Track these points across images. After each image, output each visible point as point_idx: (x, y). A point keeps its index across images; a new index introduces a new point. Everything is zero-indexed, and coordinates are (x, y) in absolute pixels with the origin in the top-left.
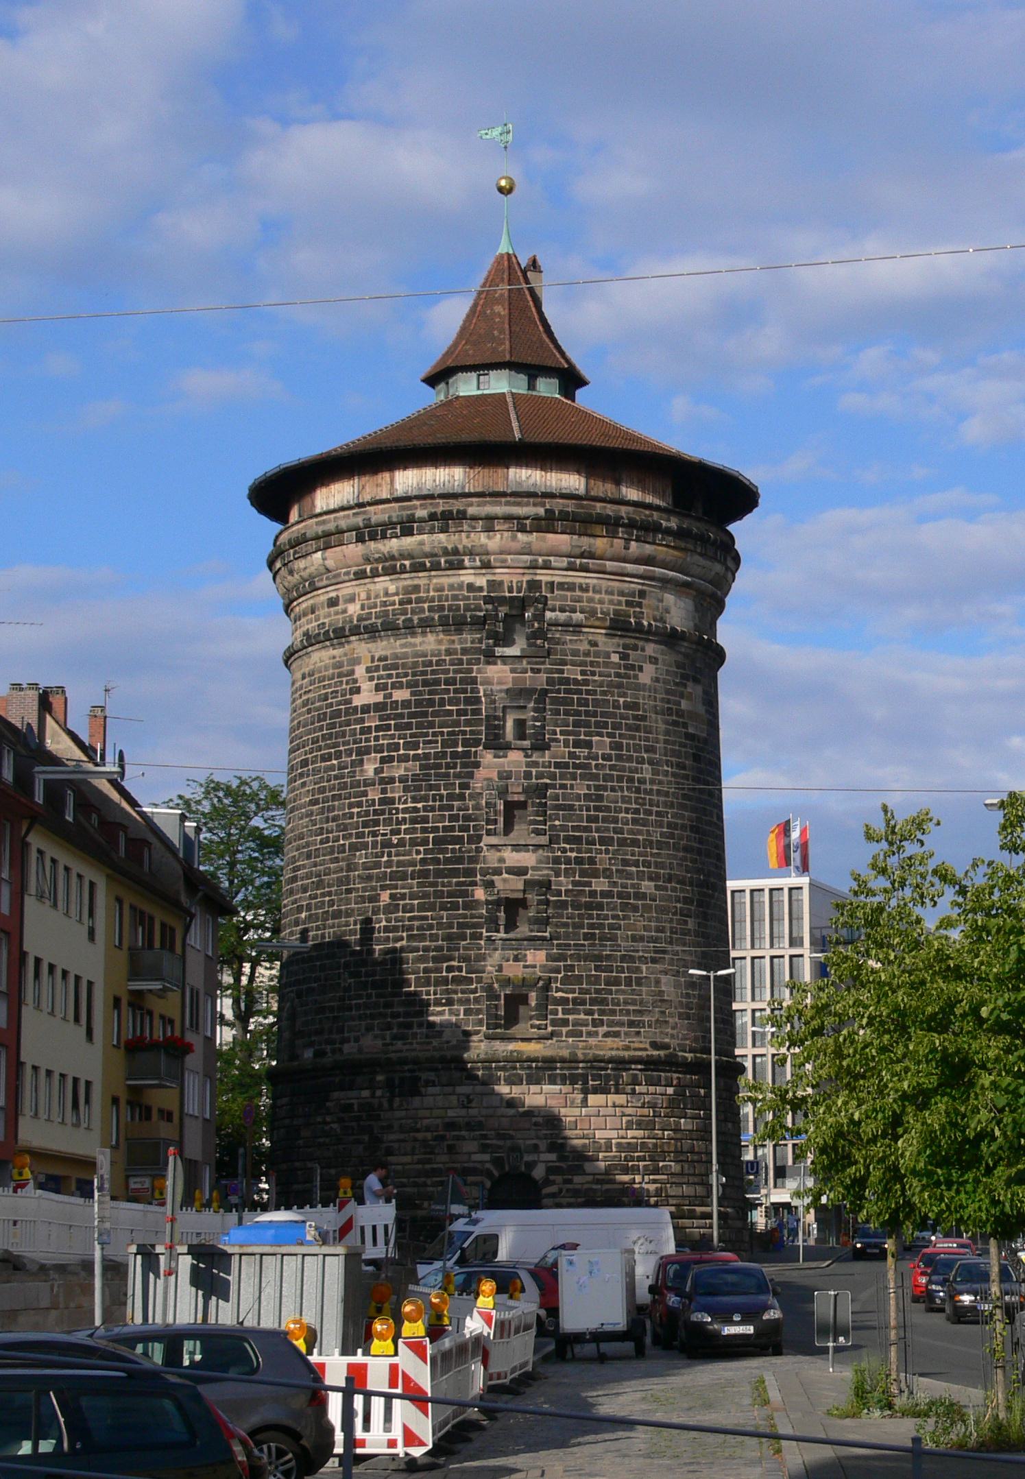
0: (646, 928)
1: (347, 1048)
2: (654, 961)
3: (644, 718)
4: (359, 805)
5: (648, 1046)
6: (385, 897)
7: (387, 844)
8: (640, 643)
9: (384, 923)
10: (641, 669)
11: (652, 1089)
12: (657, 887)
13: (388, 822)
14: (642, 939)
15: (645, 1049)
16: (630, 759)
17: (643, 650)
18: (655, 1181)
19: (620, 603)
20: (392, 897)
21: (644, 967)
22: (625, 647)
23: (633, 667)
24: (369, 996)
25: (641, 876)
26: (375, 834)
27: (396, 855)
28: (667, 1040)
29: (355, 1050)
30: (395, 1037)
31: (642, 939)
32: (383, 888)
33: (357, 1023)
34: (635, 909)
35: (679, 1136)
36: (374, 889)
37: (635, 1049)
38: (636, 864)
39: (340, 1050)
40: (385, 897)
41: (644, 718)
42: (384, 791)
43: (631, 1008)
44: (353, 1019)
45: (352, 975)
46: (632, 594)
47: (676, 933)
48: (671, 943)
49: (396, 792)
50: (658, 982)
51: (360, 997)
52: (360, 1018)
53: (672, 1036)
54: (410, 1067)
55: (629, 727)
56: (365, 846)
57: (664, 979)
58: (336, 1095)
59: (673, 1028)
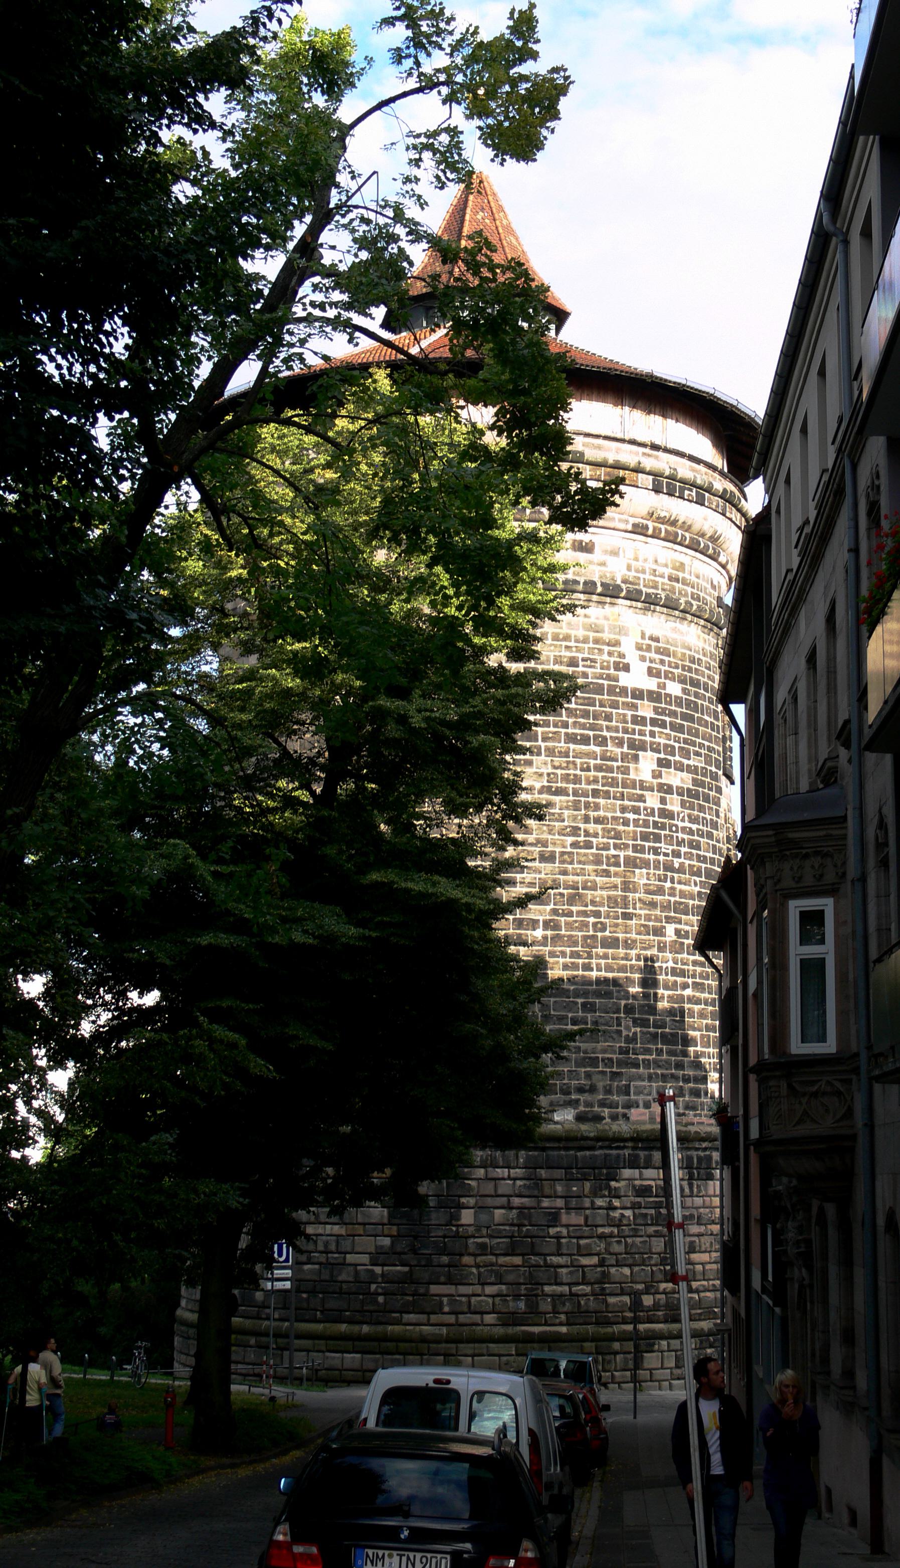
1: (635, 1114)
4: (636, 810)
6: (670, 929)
7: (669, 867)
9: (671, 964)
13: (669, 840)
20: (678, 932)
24: (659, 1052)
26: (656, 851)
27: (680, 883)
29: (647, 1117)
30: (687, 1107)
32: (669, 920)
33: (646, 1083)
36: (658, 919)
39: (626, 1117)
40: (670, 929)
42: (663, 801)
44: (640, 1078)
45: (635, 1022)
49: (674, 804)
51: (648, 1051)
52: (650, 1078)
54: (704, 1145)
56: (646, 864)
58: (627, 1173)
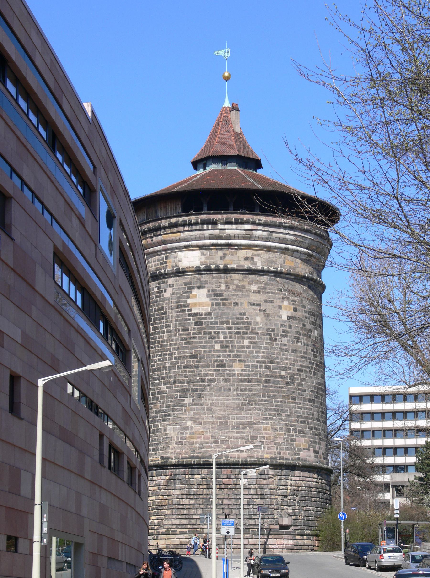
0: (161, 407)
2: (164, 420)
3: (165, 313)
5: (159, 459)
8: (165, 280)
10: (165, 291)
11: (159, 478)
12: (167, 388)
14: (159, 411)
15: (158, 460)
16: (159, 332)
17: (167, 282)
18: (157, 519)
19: (158, 265)
21: (159, 424)
22: (159, 284)
23: (162, 291)
25: (160, 384)
28: (168, 455)
31: (159, 411)
34: (157, 399)
35: (170, 497)
37: (154, 461)
38: (159, 379)
41: (165, 313)
43: (154, 443)
46: (163, 259)
47: (177, 406)
48: (173, 411)
50: (165, 430)
53: (171, 453)
55: (159, 319)
57: (168, 428)
59: (172, 449)
